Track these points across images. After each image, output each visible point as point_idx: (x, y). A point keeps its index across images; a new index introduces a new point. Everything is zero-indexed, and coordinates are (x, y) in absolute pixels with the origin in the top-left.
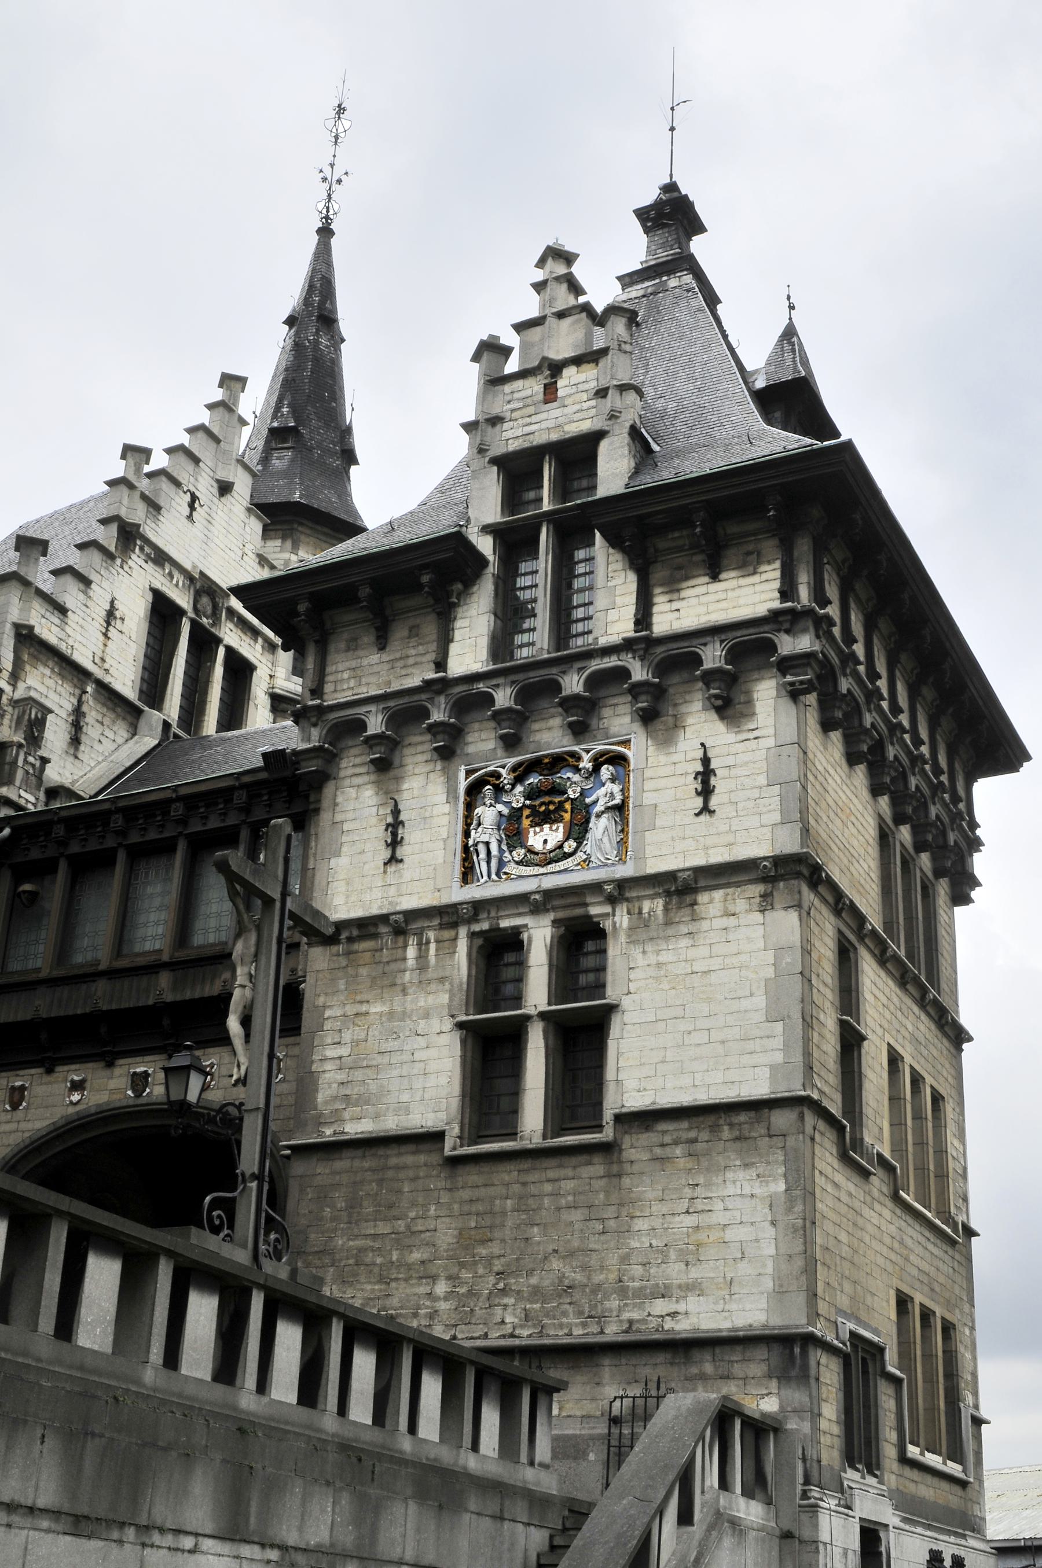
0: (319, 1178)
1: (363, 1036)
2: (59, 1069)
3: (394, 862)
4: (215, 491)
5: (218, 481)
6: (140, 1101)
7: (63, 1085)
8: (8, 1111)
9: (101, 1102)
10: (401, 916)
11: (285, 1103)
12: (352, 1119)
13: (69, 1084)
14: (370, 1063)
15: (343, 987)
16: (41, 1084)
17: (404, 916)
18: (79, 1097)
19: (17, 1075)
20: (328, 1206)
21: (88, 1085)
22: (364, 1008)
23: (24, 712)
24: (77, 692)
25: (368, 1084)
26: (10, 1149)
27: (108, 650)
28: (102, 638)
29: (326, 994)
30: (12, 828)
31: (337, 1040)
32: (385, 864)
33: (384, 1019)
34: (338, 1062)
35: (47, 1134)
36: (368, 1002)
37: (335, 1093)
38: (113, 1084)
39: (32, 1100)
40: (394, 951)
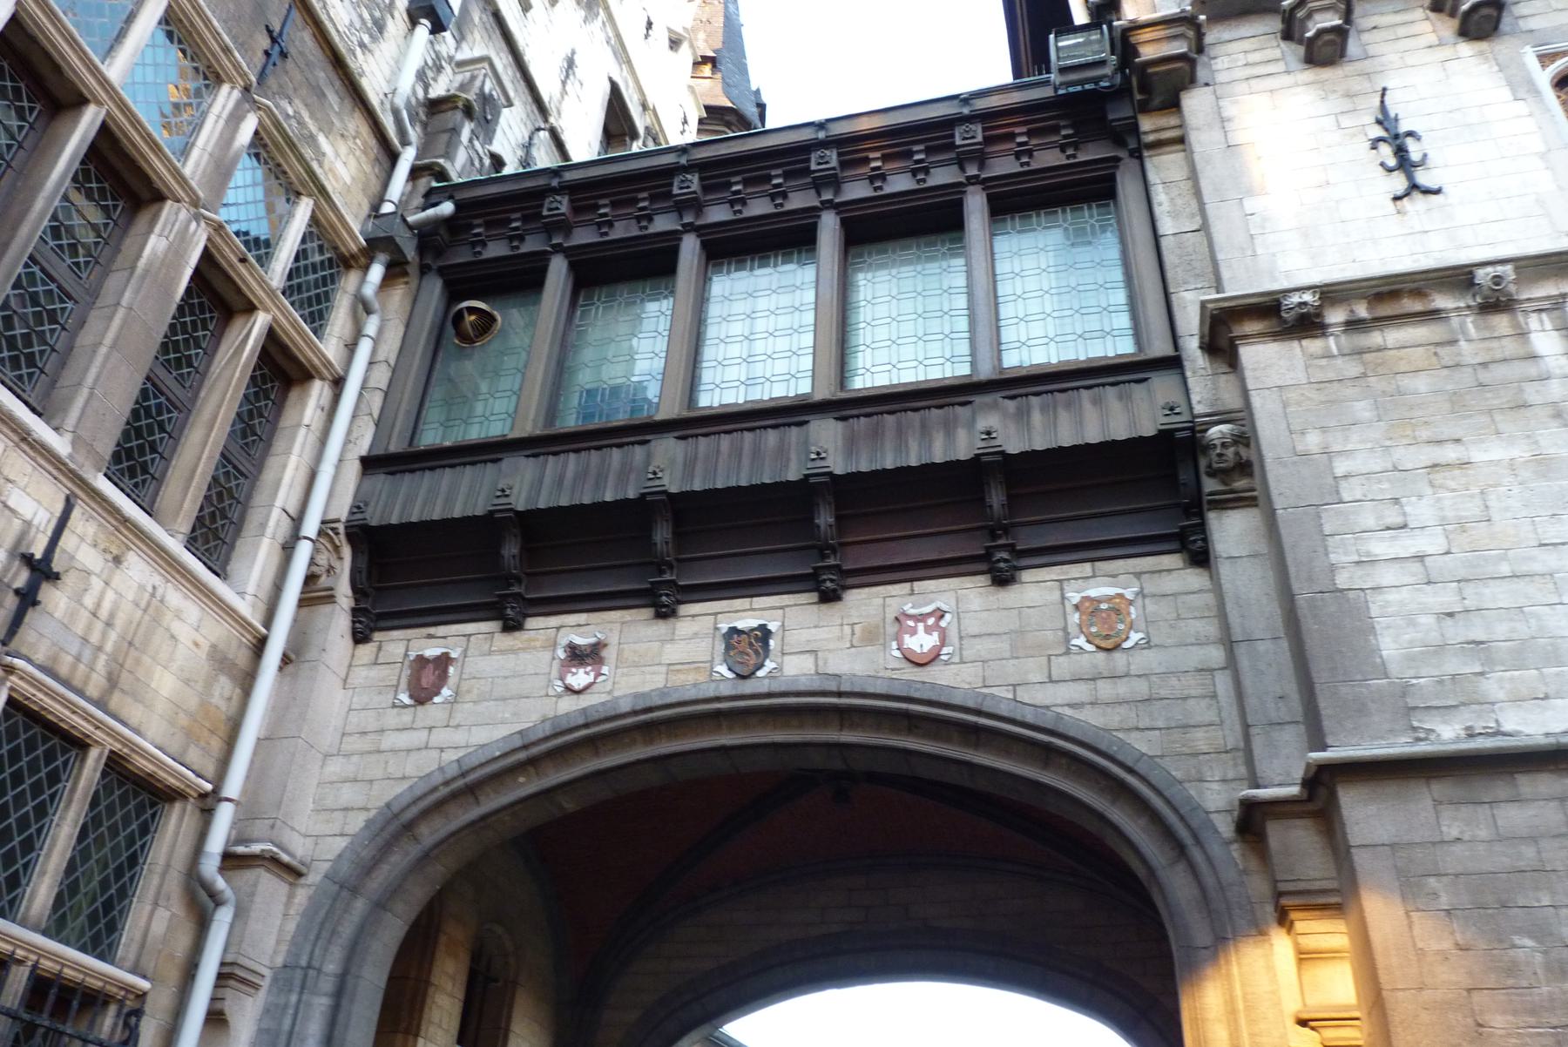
0: (1458, 849)
1: (1472, 509)
2: (532, 623)
3: (1417, 195)
4: (667, 43)
5: (670, 30)
6: (748, 687)
7: (547, 655)
8: (406, 706)
9: (647, 688)
10: (1508, 269)
11: (1163, 693)
12: (1517, 700)
13: (561, 654)
14: (1524, 568)
15: (1367, 415)
16: (490, 653)
17: (1516, 269)
18: (591, 678)
19: (430, 636)
20: (1520, 931)
21: (609, 654)
22: (1450, 453)
23: (473, 78)
24: (530, 127)
25: (1538, 617)
26: (405, 785)
27: (564, 103)
28: (559, 85)
29: (1324, 429)
30: (458, 206)
31: (1398, 520)
32: (1397, 199)
33: (1525, 474)
34: (1416, 567)
35: (505, 755)
36: (1458, 441)
37: (1434, 637)
38: (674, 653)
39: (465, 686)
40: (1495, 344)
